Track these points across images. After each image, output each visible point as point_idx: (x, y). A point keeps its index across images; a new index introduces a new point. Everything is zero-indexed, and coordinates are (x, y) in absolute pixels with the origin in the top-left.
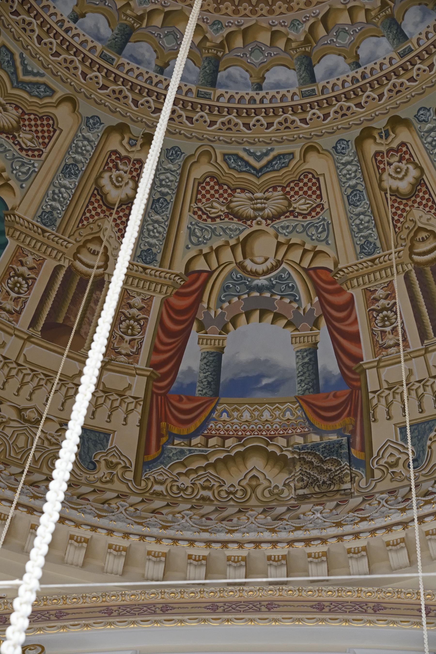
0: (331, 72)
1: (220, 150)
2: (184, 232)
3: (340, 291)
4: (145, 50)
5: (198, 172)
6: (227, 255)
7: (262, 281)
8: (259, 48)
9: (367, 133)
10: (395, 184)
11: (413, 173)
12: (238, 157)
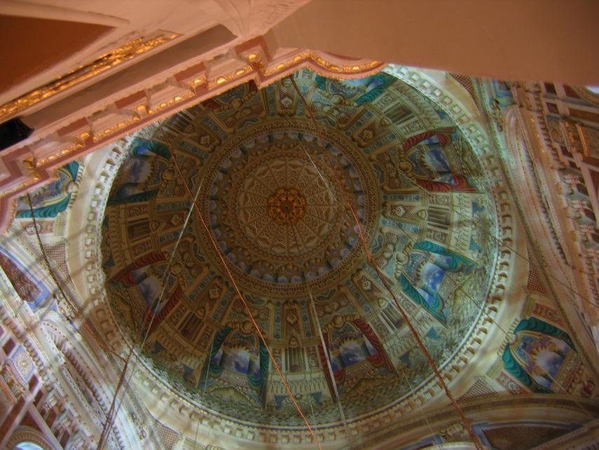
0: (237, 153)
1: (260, 121)
2: (262, 97)
3: (209, 107)
4: (292, 137)
5: (263, 114)
6: (246, 98)
7: (233, 97)
8: (260, 150)
9: (220, 144)
10: (205, 137)
11: (202, 142)
12: (254, 121)
